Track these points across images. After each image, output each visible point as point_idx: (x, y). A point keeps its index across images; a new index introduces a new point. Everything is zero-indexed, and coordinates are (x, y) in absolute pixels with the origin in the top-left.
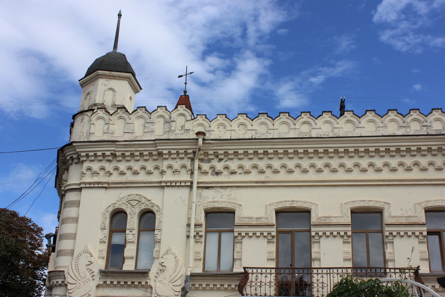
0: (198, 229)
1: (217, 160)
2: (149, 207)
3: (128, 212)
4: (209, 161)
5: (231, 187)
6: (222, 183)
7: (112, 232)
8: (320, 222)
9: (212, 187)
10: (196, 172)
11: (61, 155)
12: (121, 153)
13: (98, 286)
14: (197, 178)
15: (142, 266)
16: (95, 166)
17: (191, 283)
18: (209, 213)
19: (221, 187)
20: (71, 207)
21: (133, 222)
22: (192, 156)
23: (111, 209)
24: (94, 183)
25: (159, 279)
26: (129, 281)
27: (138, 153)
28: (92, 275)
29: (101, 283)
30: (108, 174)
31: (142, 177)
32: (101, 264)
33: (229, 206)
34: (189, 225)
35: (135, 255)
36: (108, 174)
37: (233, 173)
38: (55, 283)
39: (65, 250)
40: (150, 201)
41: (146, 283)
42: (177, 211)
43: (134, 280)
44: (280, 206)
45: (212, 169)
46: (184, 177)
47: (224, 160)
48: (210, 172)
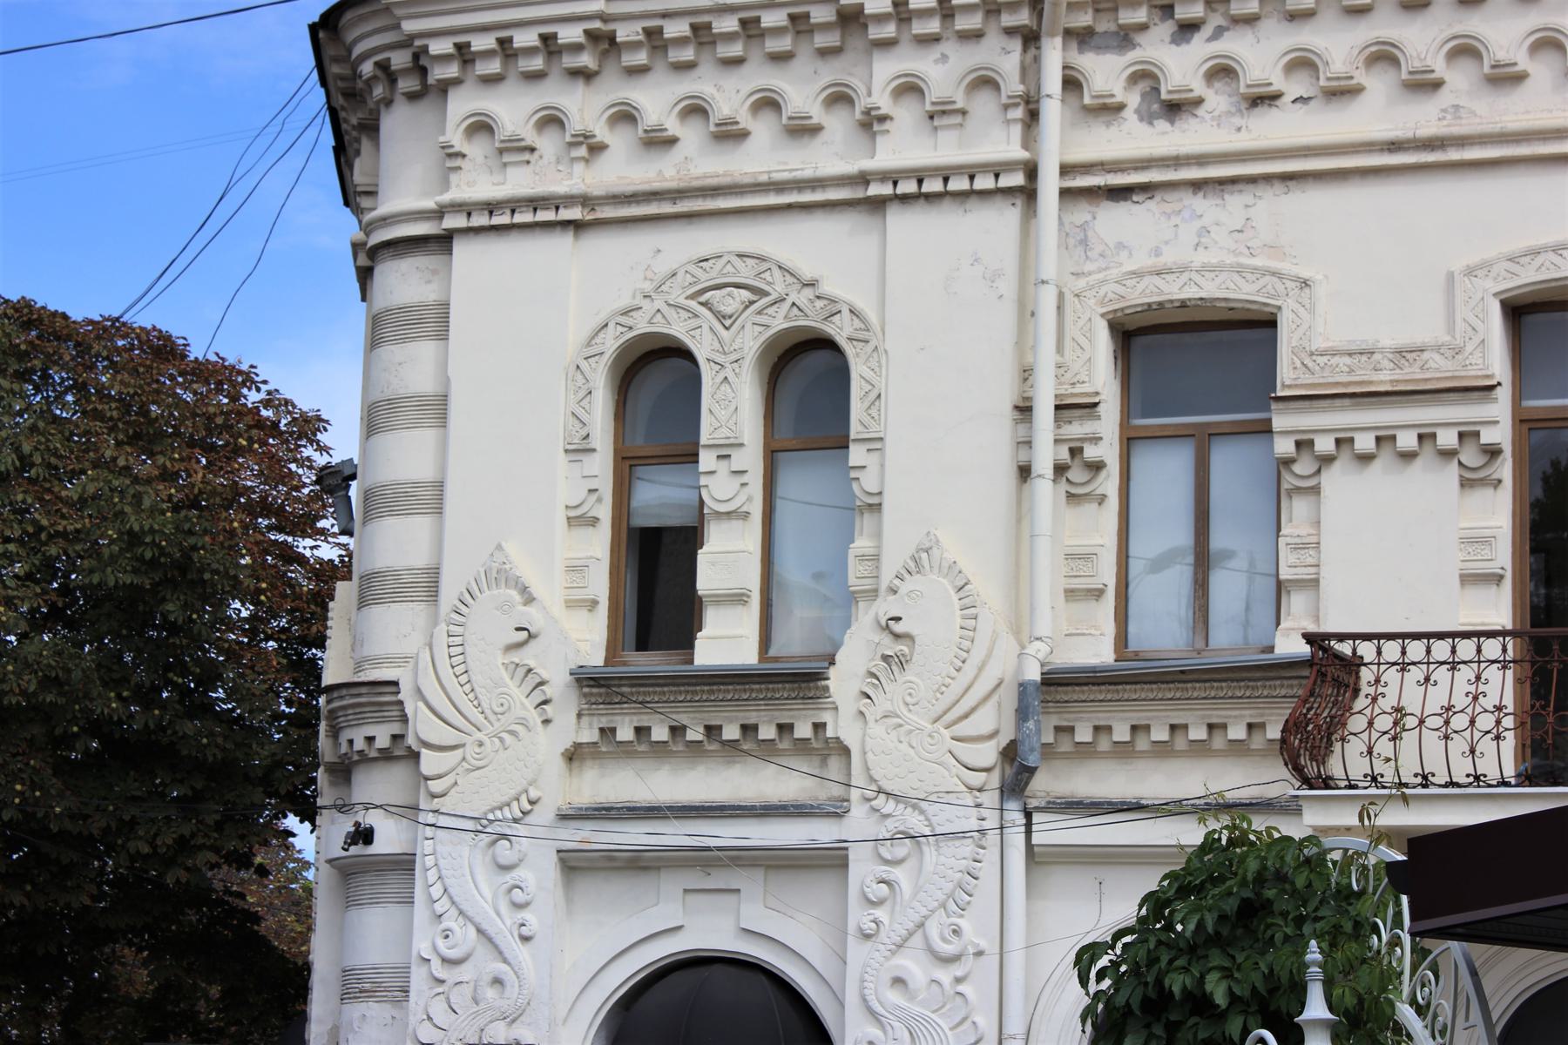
0: (1076, 429)
1: (1165, 29)
2: (813, 321)
3: (701, 355)
4: (1125, 38)
5: (1252, 180)
6: (1201, 160)
7: (628, 465)
9: (1147, 189)
10: (1053, 110)
11: (329, 51)
12: (638, 26)
13: (574, 755)
14: (1062, 140)
15: (793, 642)
16: (513, 109)
17: (1055, 721)
18: (1135, 336)
19: (1197, 186)
20: (404, 340)
21: (732, 407)
23: (611, 343)
24: (513, 205)
25: (882, 703)
26: (731, 721)
27: (729, 24)
28: (538, 697)
29: (589, 735)
30: (582, 151)
31: (764, 156)
32: (586, 638)
34: (1024, 410)
35: (753, 583)
36: (582, 151)
37: (1262, 99)
38: (359, 744)
39: (395, 573)
40: (811, 284)
41: (819, 727)
42: (965, 338)
43: (751, 718)
44: (1530, 276)
45: (1144, 85)
46: (993, 140)
47: (1207, 31)
48: (1133, 99)
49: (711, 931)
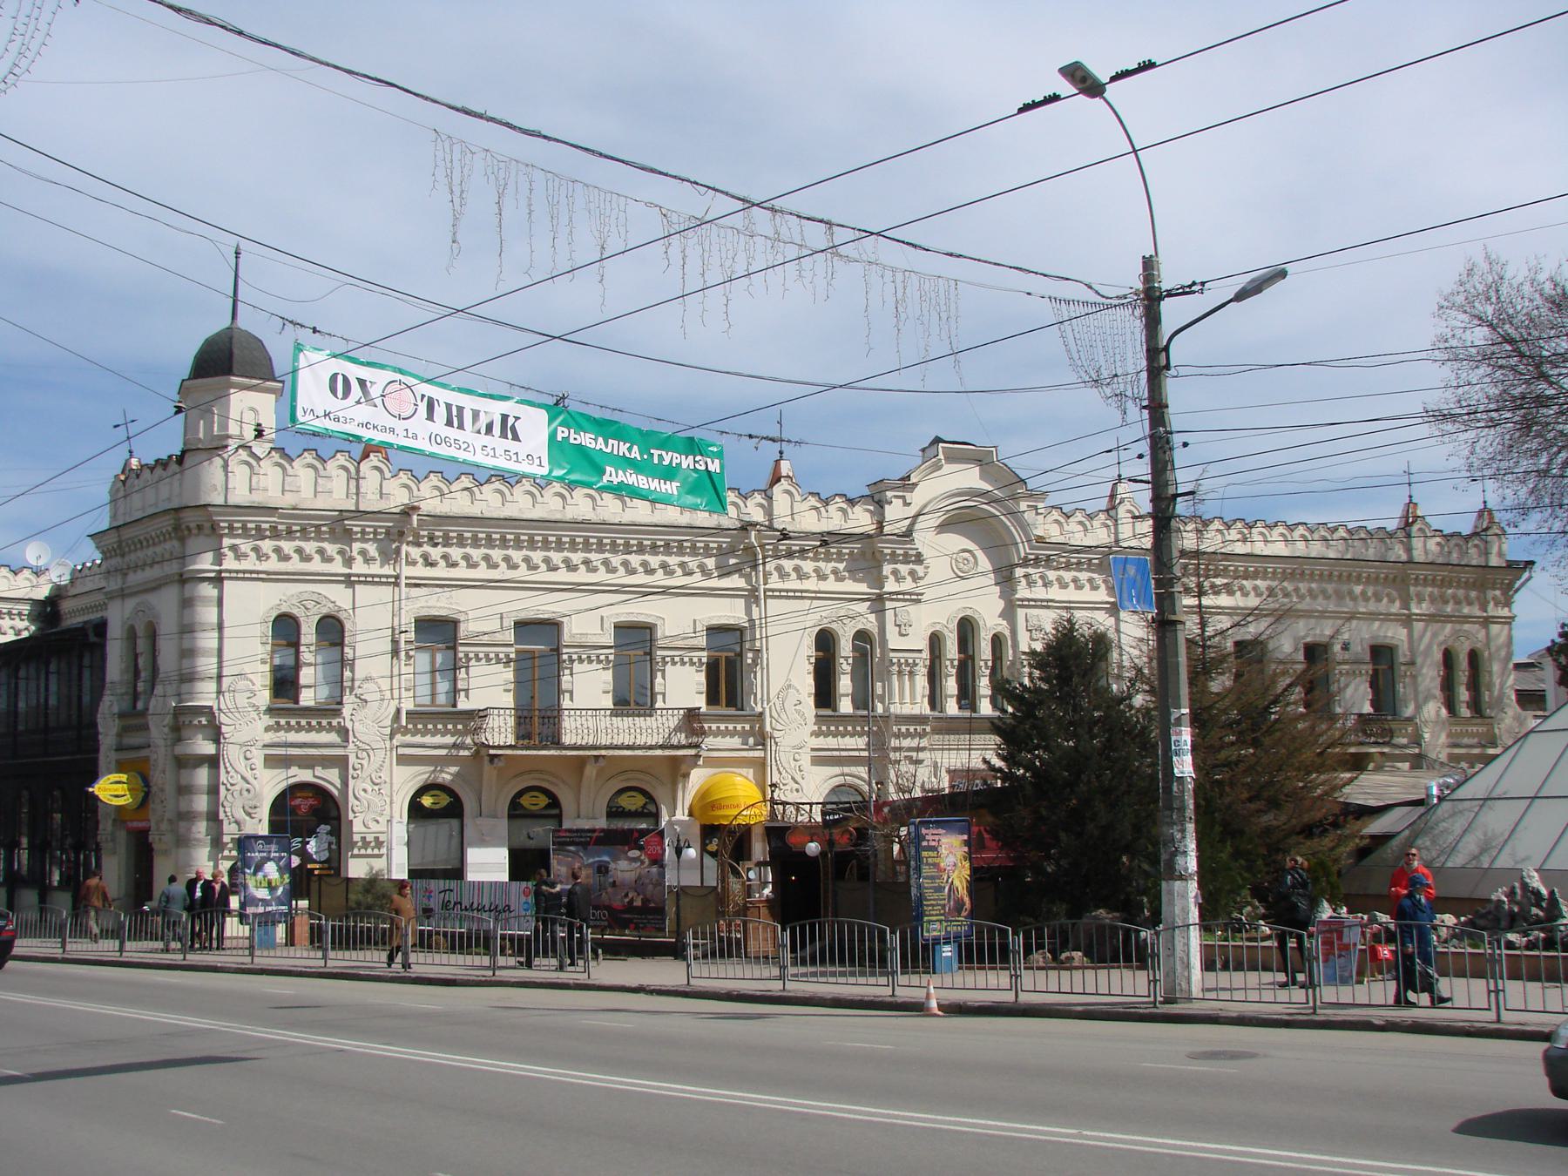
4: (419, 545)
8: (577, 641)
13: (267, 729)
21: (308, 634)
24: (244, 572)
31: (316, 565)
32: (264, 697)
44: (523, 616)
49: (305, 776)
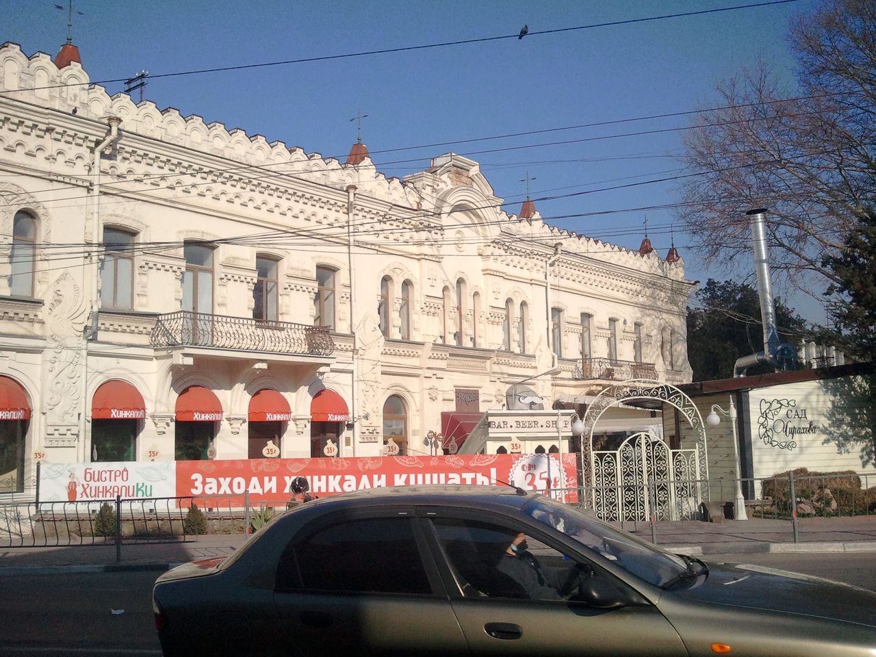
22: (93, 145)
25: (55, 311)
26: (12, 311)
33: (132, 225)
43: (17, 311)
46: (79, 170)
